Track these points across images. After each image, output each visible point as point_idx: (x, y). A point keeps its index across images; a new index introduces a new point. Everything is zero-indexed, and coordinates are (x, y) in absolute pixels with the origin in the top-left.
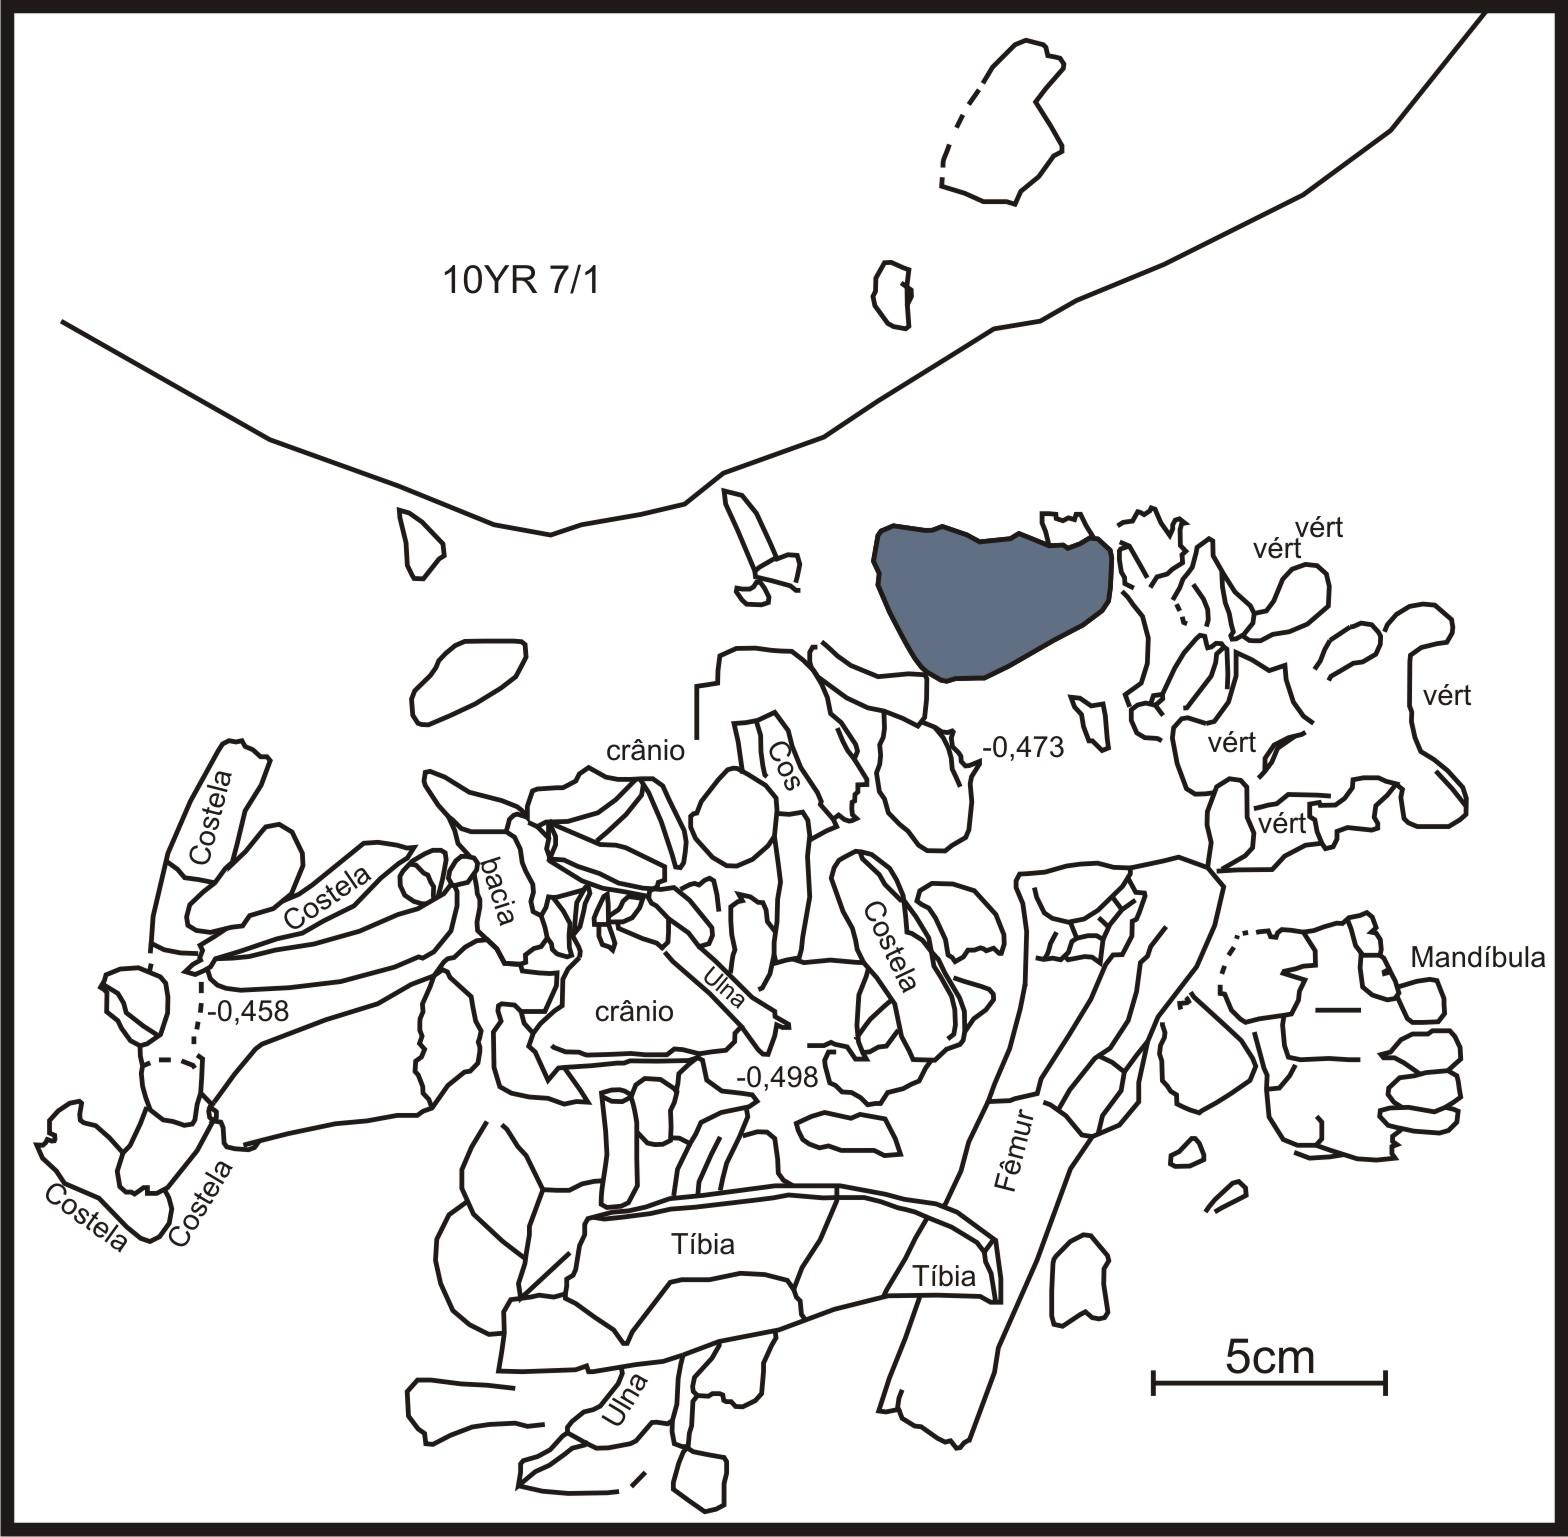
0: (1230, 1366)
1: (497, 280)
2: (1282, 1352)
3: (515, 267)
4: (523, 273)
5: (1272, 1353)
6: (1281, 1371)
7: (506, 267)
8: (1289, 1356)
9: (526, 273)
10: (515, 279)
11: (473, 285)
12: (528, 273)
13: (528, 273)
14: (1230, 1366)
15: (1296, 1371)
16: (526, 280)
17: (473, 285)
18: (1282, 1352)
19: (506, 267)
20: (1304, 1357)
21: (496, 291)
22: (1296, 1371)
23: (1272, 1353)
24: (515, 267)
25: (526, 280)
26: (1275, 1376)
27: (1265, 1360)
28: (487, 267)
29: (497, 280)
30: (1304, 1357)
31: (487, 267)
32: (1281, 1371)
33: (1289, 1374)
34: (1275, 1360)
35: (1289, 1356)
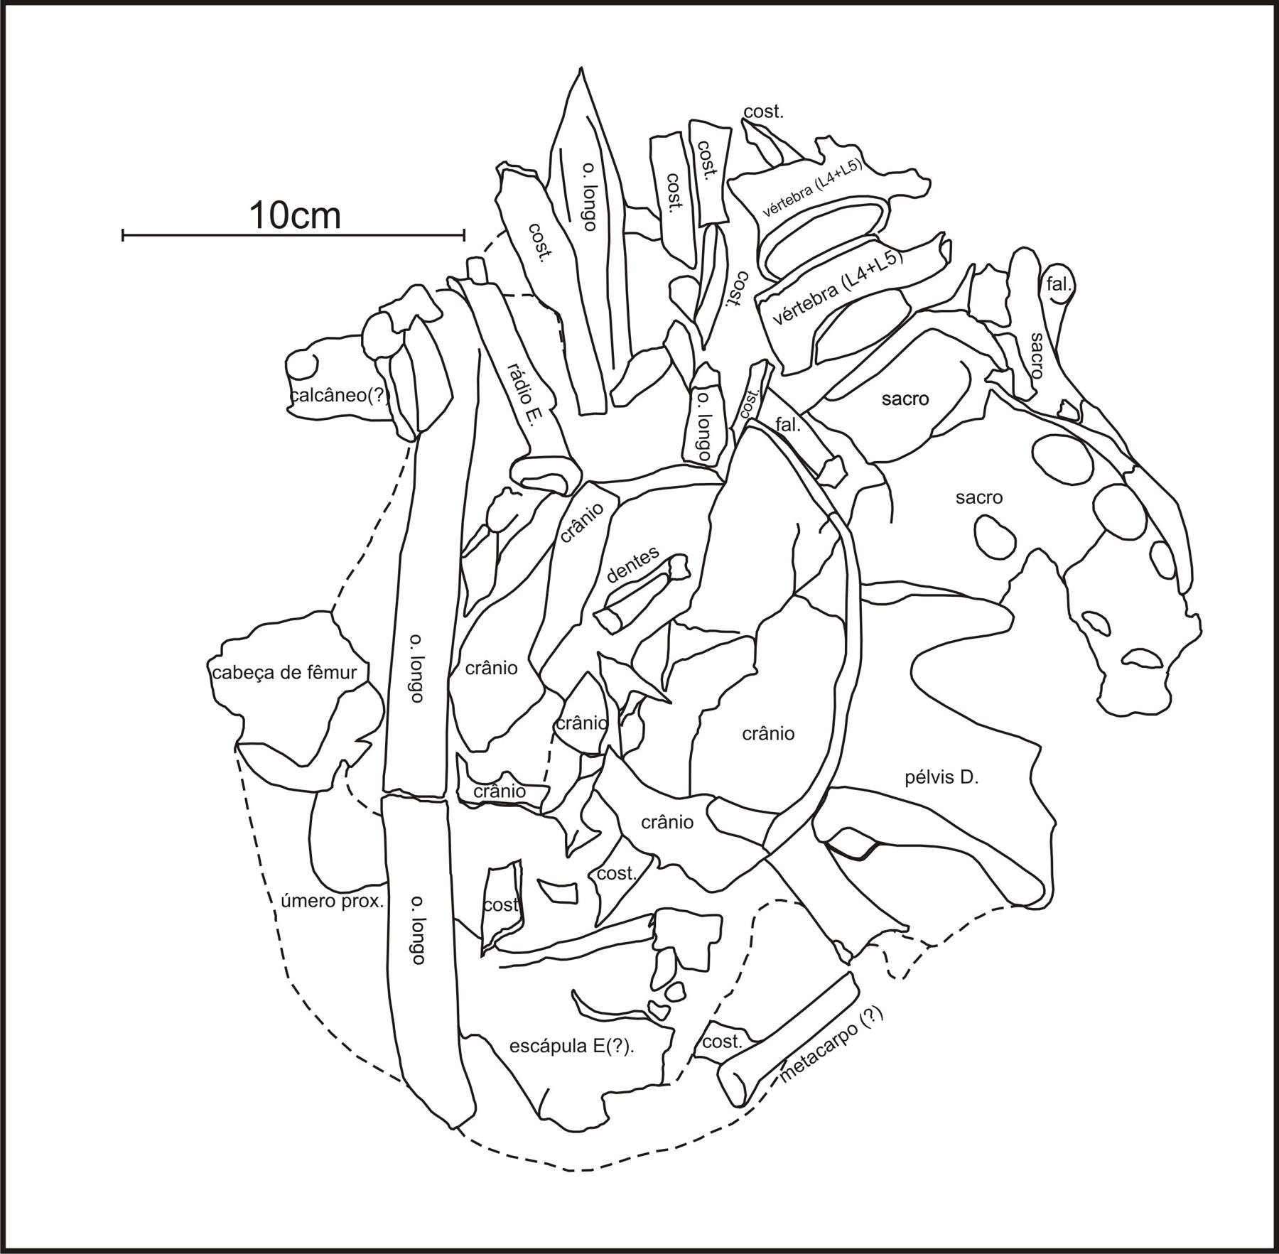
2: (315, 212)
5: (307, 212)
6: (314, 226)
8: (320, 215)
15: (326, 226)
18: (315, 212)
20: (332, 215)
22: (326, 226)
23: (307, 212)
26: (309, 230)
27: (301, 218)
30: (332, 215)
32: (314, 226)
33: (320, 229)
34: (309, 218)
35: (320, 215)
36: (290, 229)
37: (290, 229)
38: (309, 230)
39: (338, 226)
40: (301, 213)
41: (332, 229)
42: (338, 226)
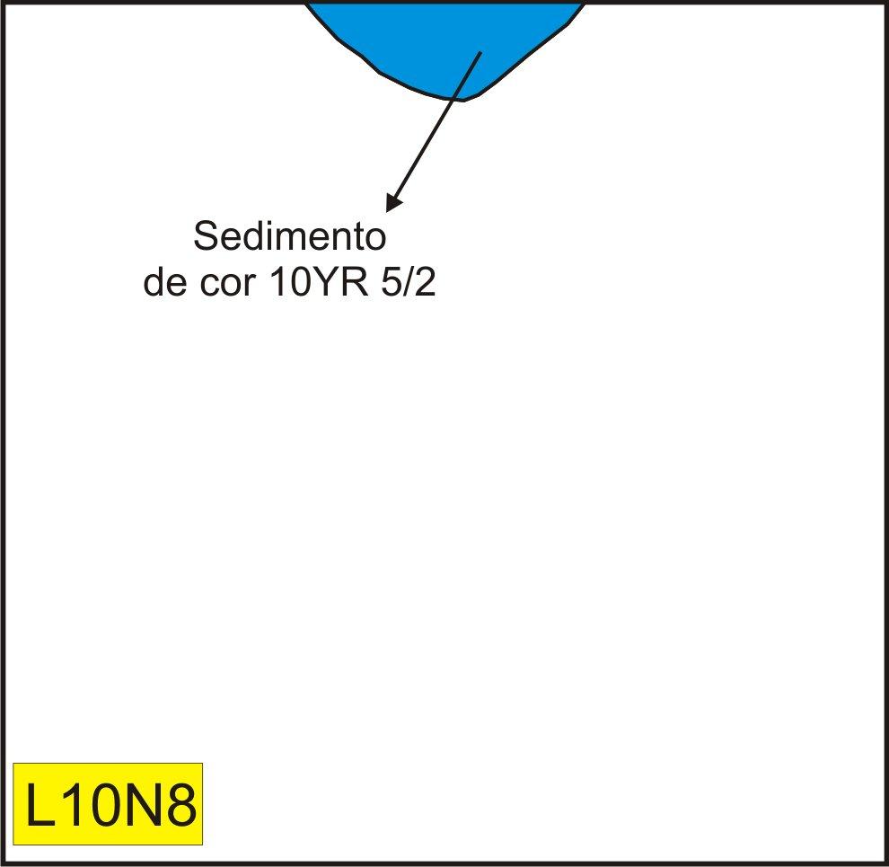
0: (384, 290)
1: (326, 282)
3: (345, 269)
4: (352, 275)
7: (336, 268)
9: (356, 275)
10: (345, 281)
11: (301, 287)
12: (358, 275)
13: (358, 275)
14: (384, 290)
16: (356, 282)
17: (301, 287)
19: (336, 268)
21: (326, 293)
24: (345, 269)
25: (356, 282)
28: (316, 269)
29: (326, 282)
31: (316, 269)
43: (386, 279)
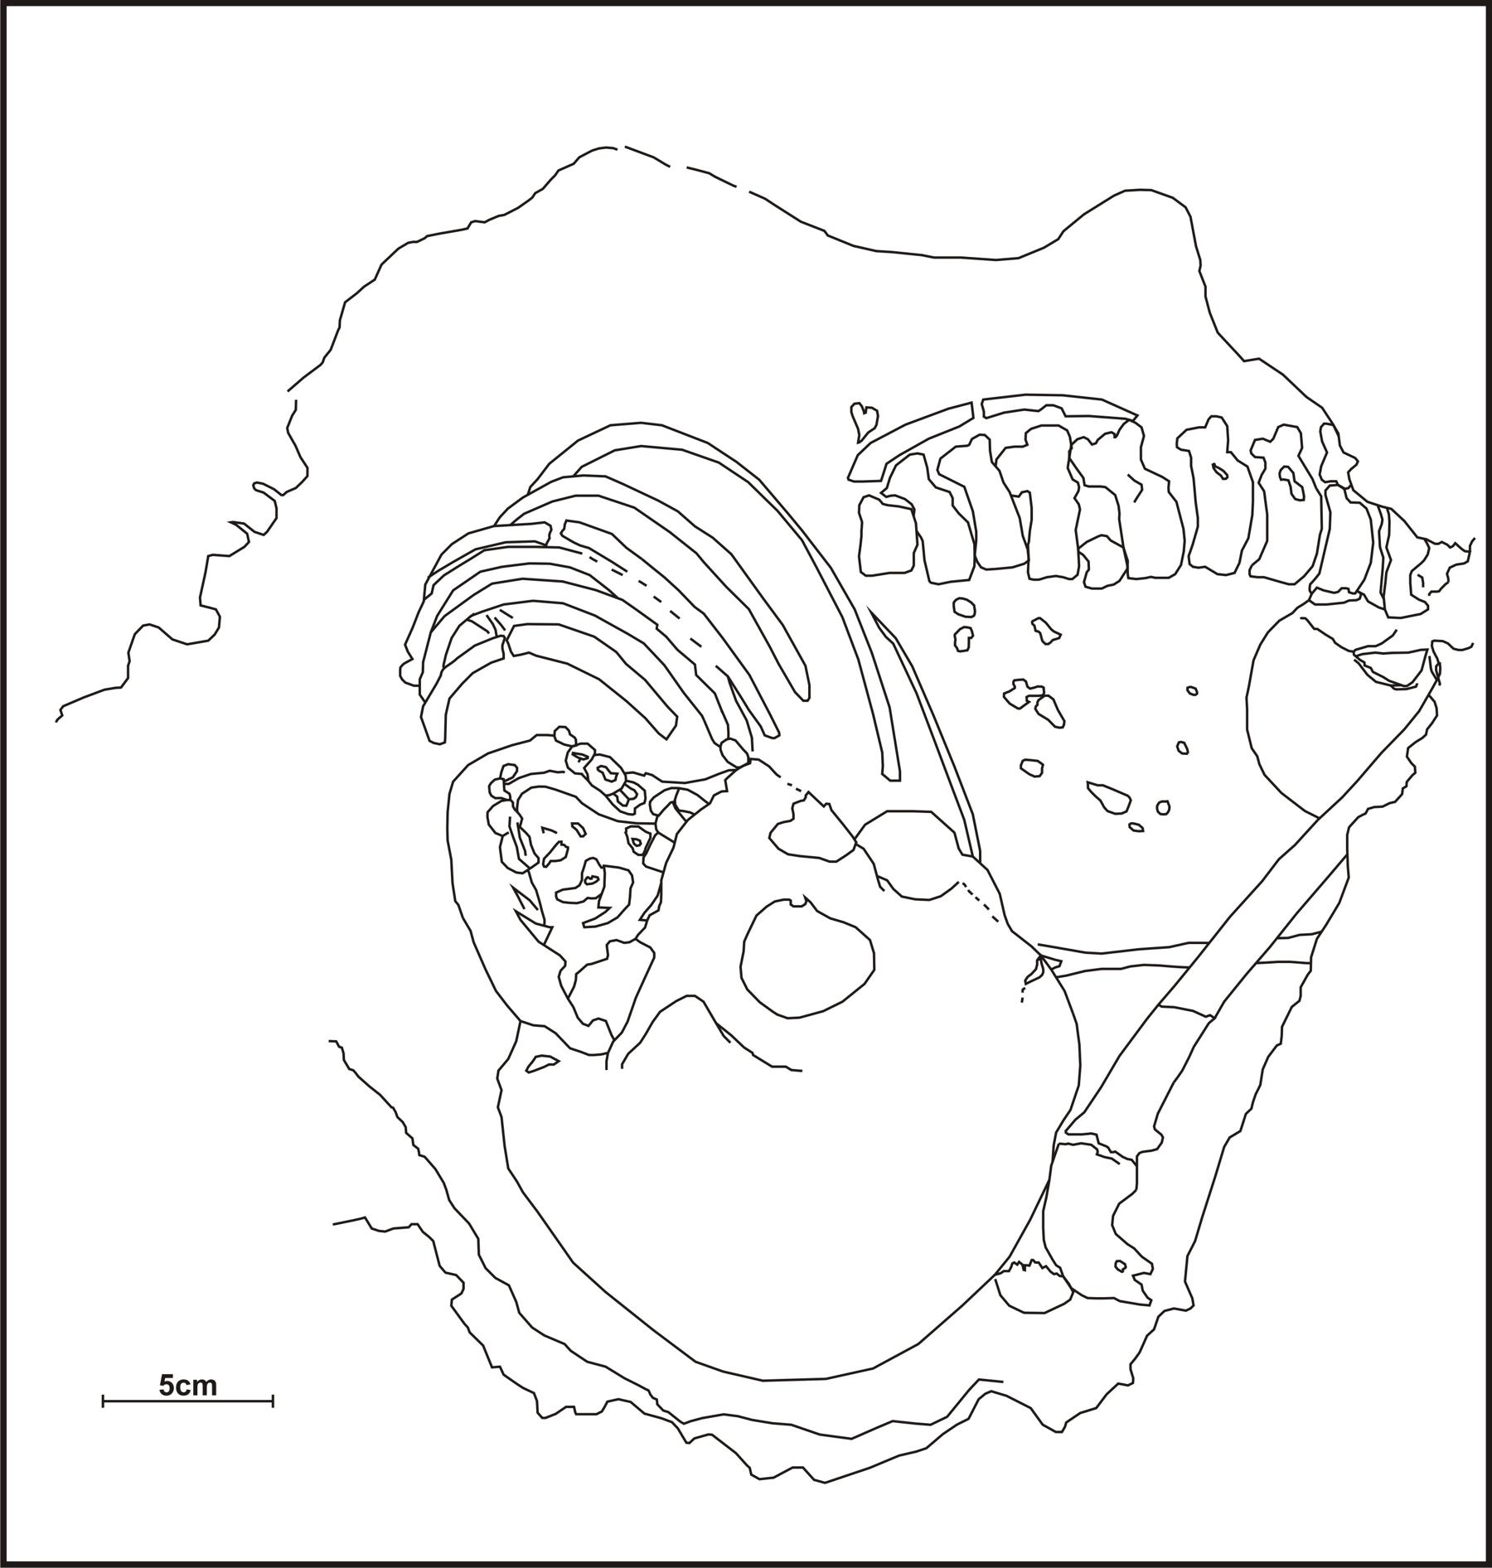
8: (200, 1386)
18: (196, 1383)
20: (210, 1386)
26: (191, 1396)
27: (184, 1387)
30: (210, 1386)
33: (200, 1396)
34: (191, 1387)
35: (200, 1386)
36: (175, 1395)
37: (175, 1395)
38: (191, 1396)
39: (214, 1393)
40: (184, 1387)
41: (209, 1396)
42: (214, 1393)
43: (163, 1383)
